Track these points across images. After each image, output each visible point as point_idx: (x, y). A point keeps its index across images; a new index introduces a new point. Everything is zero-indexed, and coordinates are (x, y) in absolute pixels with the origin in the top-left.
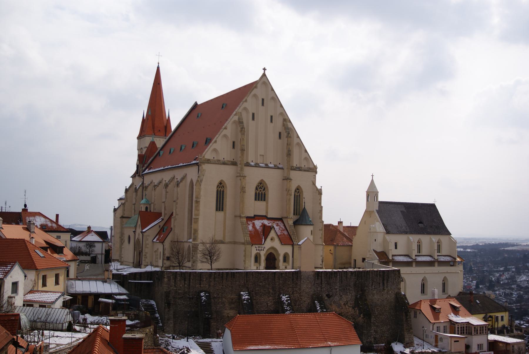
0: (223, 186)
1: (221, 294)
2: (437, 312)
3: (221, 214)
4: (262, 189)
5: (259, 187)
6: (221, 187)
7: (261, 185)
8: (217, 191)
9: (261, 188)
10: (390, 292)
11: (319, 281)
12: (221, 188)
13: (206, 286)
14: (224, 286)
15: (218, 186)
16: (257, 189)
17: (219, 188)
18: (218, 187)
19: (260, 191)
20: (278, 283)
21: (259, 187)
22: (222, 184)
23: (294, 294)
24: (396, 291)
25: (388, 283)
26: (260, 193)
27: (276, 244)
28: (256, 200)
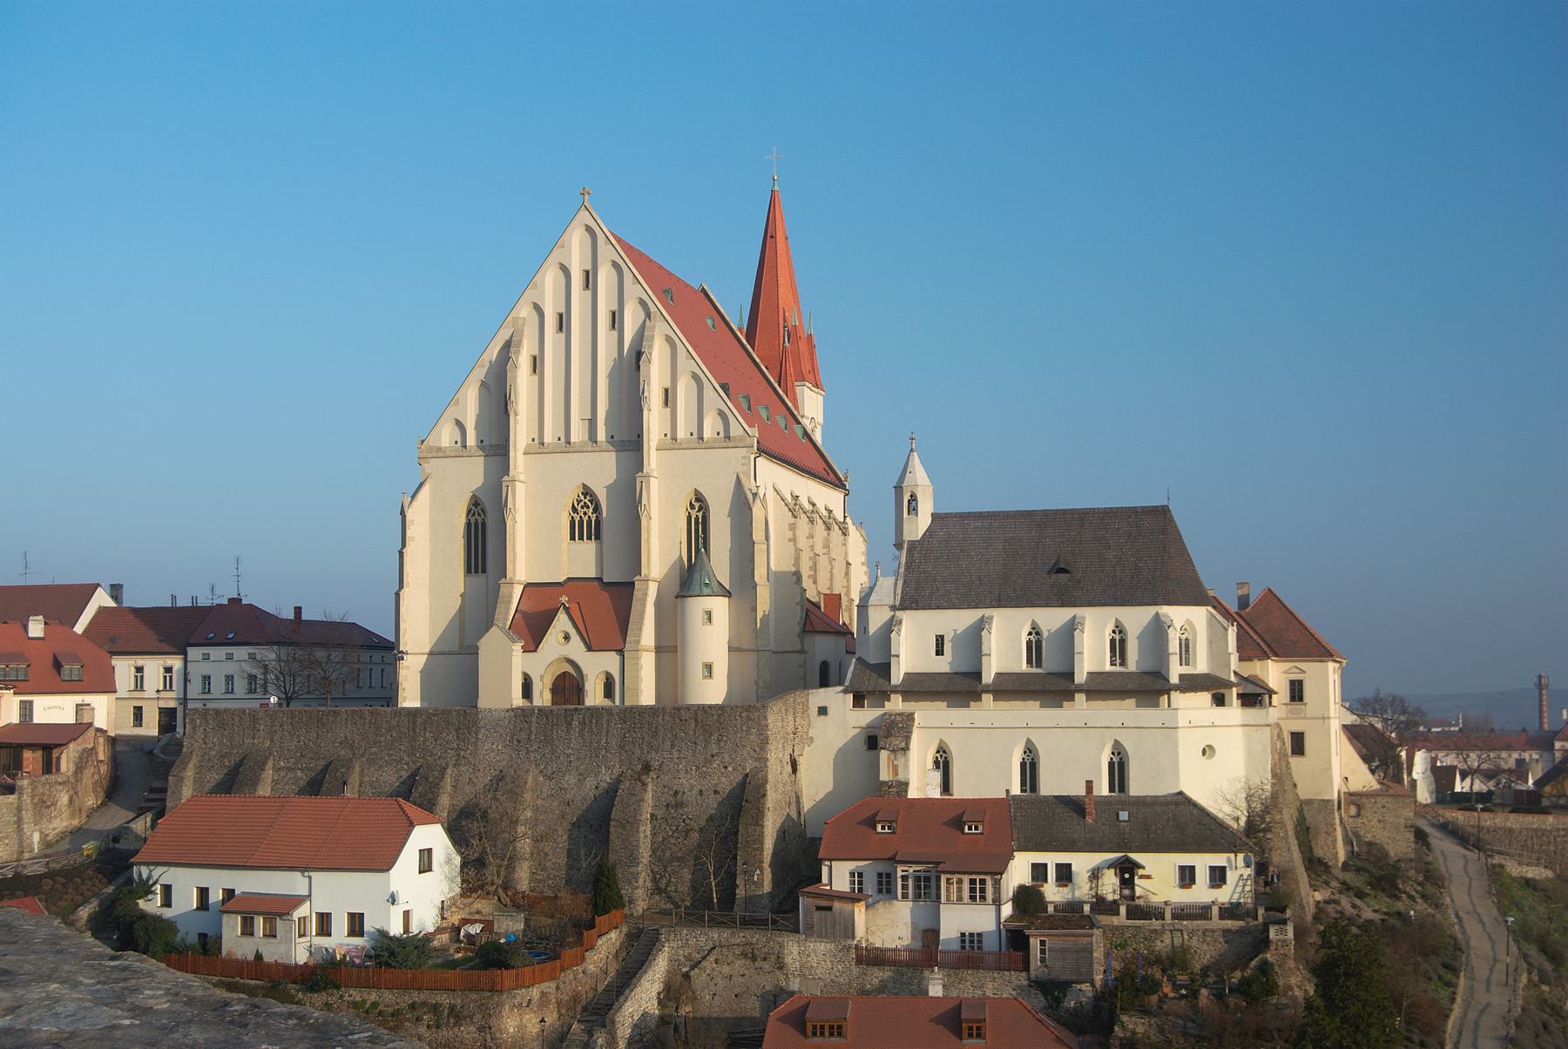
0: (483, 511)
1: (294, 760)
2: (878, 833)
3: (479, 579)
4: (591, 510)
5: (582, 503)
6: (476, 514)
7: (585, 498)
8: (468, 524)
9: (588, 507)
10: (730, 769)
11: (523, 735)
12: (479, 515)
13: (265, 741)
14: (302, 743)
15: (469, 511)
16: (574, 509)
17: (474, 515)
18: (470, 515)
19: (585, 514)
20: (422, 739)
21: (582, 503)
22: (479, 505)
23: (459, 765)
24: (749, 766)
25: (722, 744)
26: (585, 519)
27: (576, 649)
28: (572, 538)
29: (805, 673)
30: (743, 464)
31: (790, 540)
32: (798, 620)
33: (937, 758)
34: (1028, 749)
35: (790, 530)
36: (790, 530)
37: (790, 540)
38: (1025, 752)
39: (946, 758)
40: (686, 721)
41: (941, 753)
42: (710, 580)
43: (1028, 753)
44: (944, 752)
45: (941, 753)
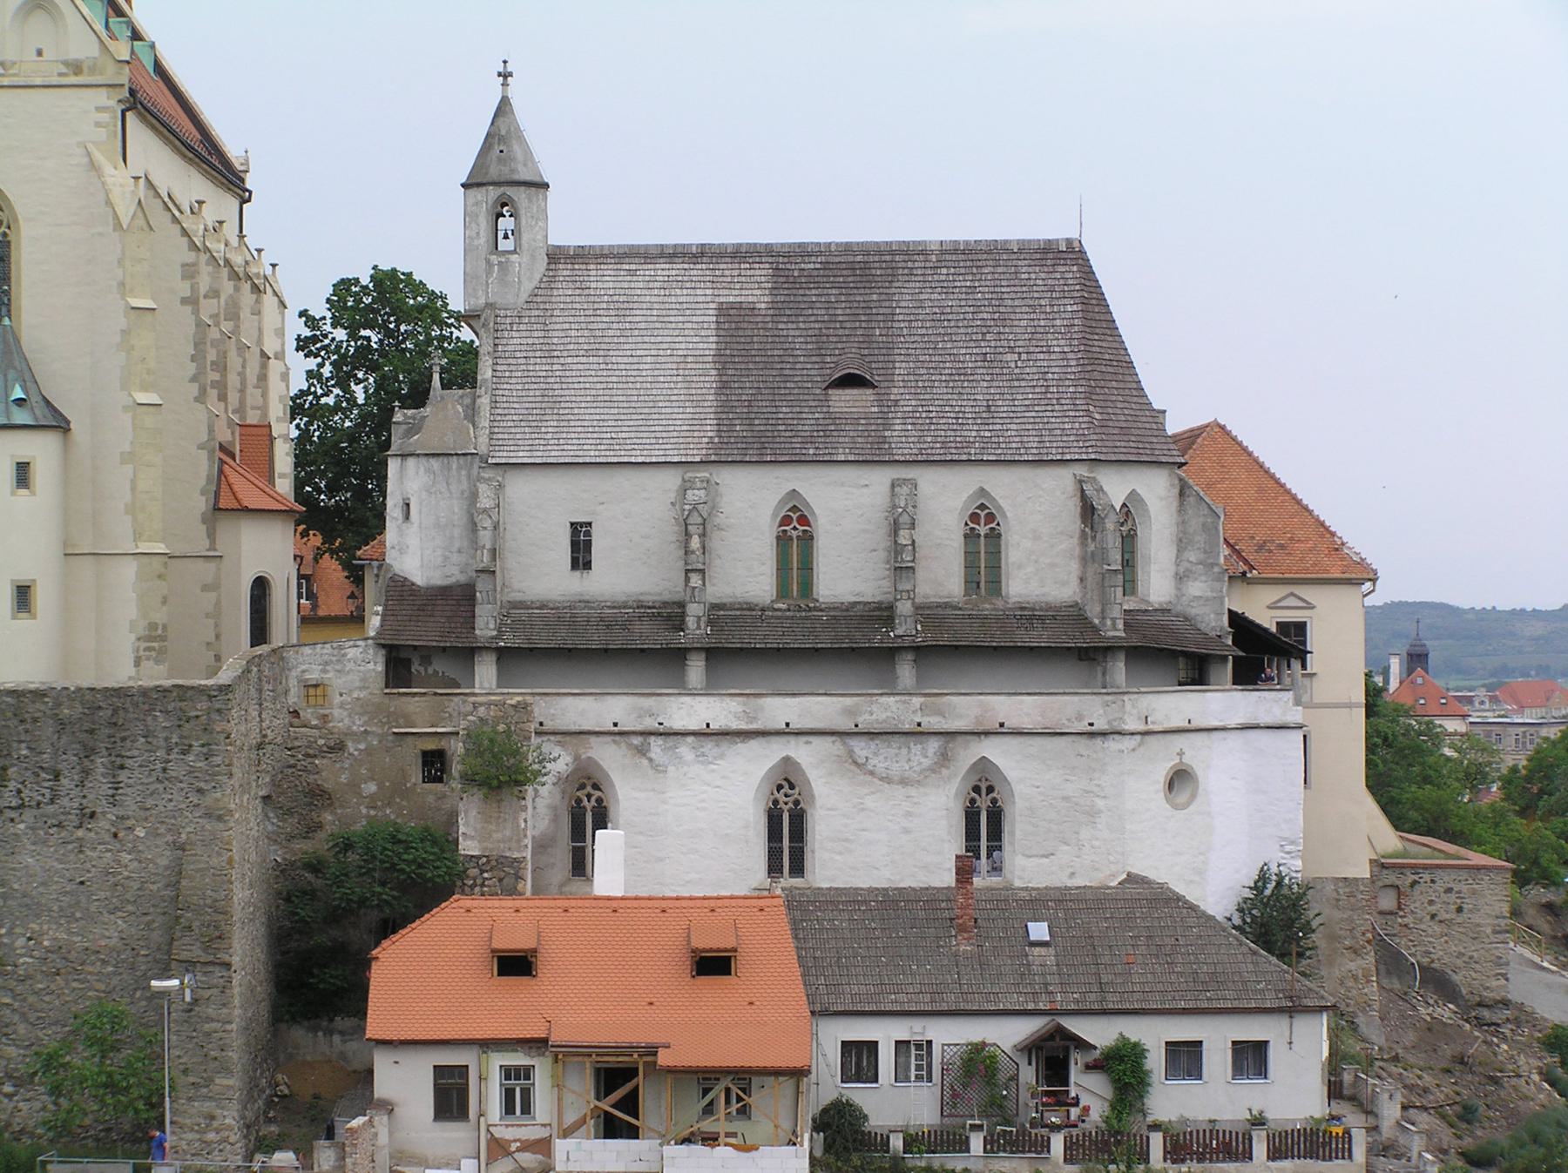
29: (218, 603)
30: (98, 124)
31: (184, 301)
32: (203, 482)
33: (579, 801)
34: (786, 779)
35: (184, 277)
36: (184, 277)
37: (184, 301)
38: (780, 787)
39: (600, 800)
40: (35, 720)
41: (589, 789)
42: (26, 392)
43: (786, 789)
44: (596, 787)
45: (589, 789)
